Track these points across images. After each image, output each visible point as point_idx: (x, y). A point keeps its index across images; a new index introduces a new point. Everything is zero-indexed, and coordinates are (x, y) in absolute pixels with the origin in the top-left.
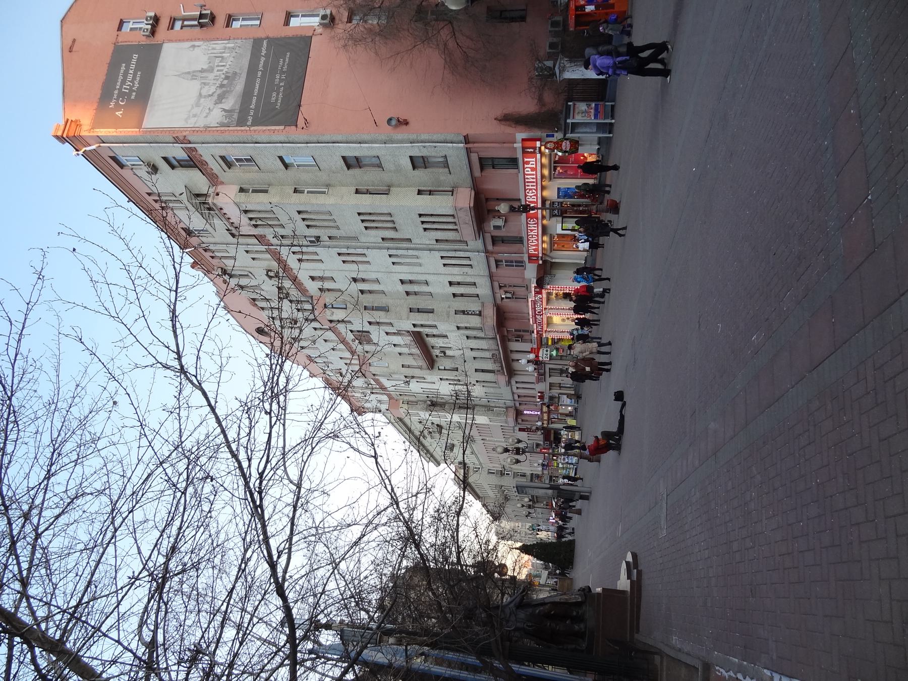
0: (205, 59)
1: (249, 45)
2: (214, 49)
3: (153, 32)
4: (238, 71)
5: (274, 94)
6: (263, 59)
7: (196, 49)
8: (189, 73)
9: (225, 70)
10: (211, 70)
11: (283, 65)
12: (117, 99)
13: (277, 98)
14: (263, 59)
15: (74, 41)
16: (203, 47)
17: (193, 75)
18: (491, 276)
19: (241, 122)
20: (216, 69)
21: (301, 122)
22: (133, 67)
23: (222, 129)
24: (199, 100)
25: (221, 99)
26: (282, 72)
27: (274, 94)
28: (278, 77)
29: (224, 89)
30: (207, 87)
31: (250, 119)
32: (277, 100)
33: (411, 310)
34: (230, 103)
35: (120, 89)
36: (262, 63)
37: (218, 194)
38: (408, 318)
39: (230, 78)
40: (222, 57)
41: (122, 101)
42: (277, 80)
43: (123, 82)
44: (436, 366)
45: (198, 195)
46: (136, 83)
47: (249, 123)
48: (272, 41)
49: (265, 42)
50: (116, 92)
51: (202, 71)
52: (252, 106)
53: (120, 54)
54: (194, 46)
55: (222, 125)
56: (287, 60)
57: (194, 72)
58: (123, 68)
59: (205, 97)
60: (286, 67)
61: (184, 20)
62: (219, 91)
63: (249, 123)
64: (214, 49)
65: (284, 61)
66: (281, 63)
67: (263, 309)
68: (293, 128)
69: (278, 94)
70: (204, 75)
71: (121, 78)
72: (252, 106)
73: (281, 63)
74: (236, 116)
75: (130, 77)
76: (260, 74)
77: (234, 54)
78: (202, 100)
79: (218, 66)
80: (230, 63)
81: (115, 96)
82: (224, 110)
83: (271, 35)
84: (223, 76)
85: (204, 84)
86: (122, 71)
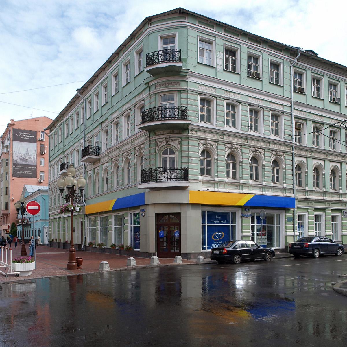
0: (32, 154)
1: (35, 164)
2: (34, 155)
5: (21, 171)
6: (31, 168)
8: (28, 150)
10: (28, 155)
12: (21, 134)
14: (31, 168)
15: (39, 121)
17: (27, 151)
19: (14, 164)
21: (14, 178)
22: (30, 136)
25: (21, 159)
26: (27, 172)
27: (21, 171)
34: (19, 161)
35: (24, 134)
37: (5, 154)
43: (26, 135)
46: (26, 138)
48: (36, 169)
49: (36, 168)
50: (23, 133)
51: (28, 154)
53: (34, 133)
54: (35, 151)
55: (13, 160)
58: (30, 134)
62: (22, 158)
63: (13, 166)
64: (34, 155)
74: (16, 163)
75: (27, 136)
78: (20, 154)
81: (22, 133)
82: (17, 160)
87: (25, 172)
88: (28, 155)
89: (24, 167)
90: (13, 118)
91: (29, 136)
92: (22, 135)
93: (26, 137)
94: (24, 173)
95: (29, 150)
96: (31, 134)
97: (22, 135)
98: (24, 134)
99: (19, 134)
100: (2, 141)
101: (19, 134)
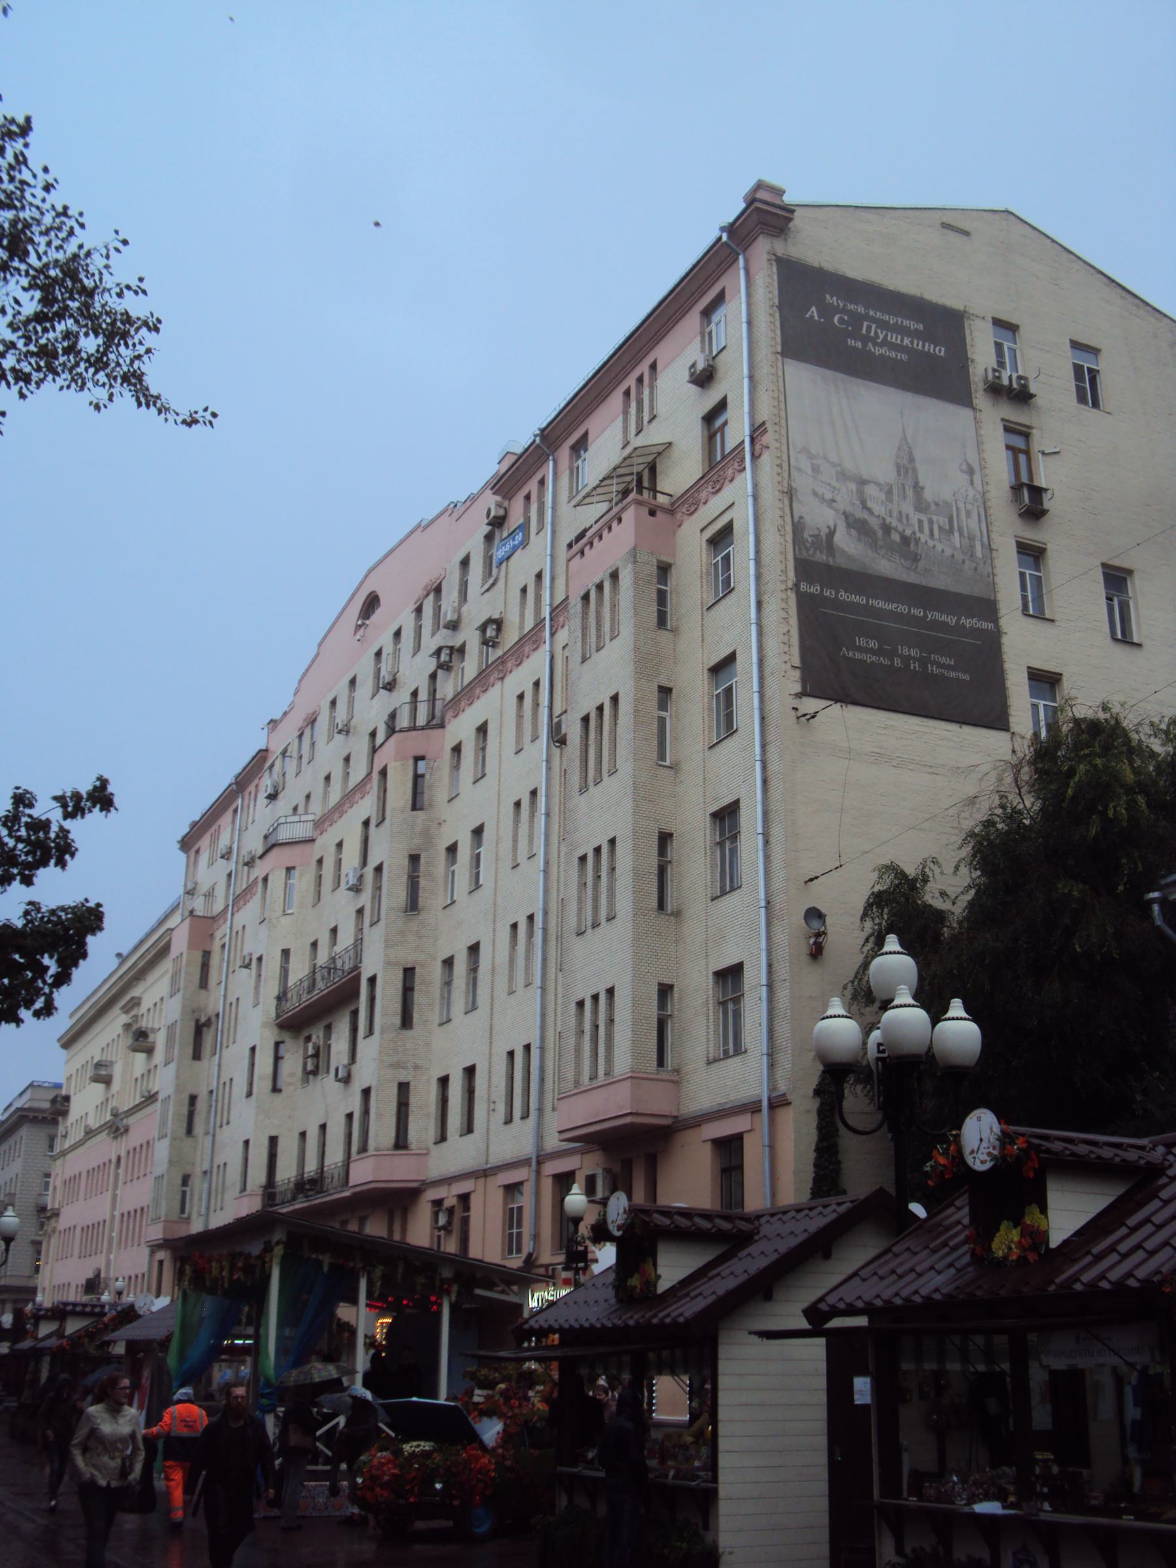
0: (946, 494)
2: (968, 514)
3: (996, 390)
4: (922, 564)
5: (873, 644)
6: (951, 620)
7: (966, 477)
8: (912, 460)
9: (924, 537)
10: (921, 506)
11: (940, 666)
12: (844, 311)
13: (864, 650)
14: (951, 620)
16: (971, 492)
17: (906, 467)
18: (484, 1174)
19: (805, 569)
20: (924, 518)
21: (811, 705)
22: (918, 345)
23: (789, 528)
26: (924, 662)
27: (873, 644)
28: (914, 652)
29: (880, 533)
30: (883, 496)
31: (815, 589)
33: (409, 972)
35: (866, 317)
36: (944, 618)
38: (388, 963)
39: (906, 547)
40: (951, 531)
41: (841, 320)
42: (906, 652)
44: (286, 1037)
45: (653, 468)
46: (883, 351)
47: (803, 586)
50: (861, 309)
51: (918, 489)
52: (843, 595)
53: (946, 324)
54: (971, 472)
56: (953, 674)
57: (915, 470)
60: (936, 671)
61: (1027, 453)
62: (874, 523)
63: (803, 586)
64: (968, 514)
65: (949, 668)
66: (943, 660)
67: (419, 610)
68: (798, 688)
69: (872, 651)
70: (910, 493)
72: (843, 595)
73: (943, 660)
74: (821, 557)
75: (895, 338)
76: (919, 612)
77: (959, 556)
78: (853, 486)
79: (931, 522)
81: (851, 307)
82: (831, 534)
83: (1005, 640)
84: (908, 532)
85: (889, 492)
86: (906, 323)
87: (907, 660)
88: (921, 506)
89: (891, 607)
91: (907, 341)
92: (857, 319)
93: (885, 343)
94: (897, 662)
95: (918, 455)
96: (921, 327)
97: (857, 319)
99: (827, 311)
100: (499, 505)
101: (827, 311)
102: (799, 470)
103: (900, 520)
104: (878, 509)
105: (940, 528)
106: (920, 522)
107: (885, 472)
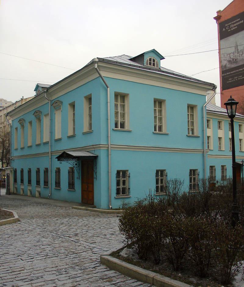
11: (240, 78)
13: (230, 81)
24: (228, 54)
27: (231, 79)
32: (230, 81)
34: (229, 66)
40: (242, 54)
59: (230, 56)
65: (241, 77)
69: (231, 80)
71: (235, 22)
75: (235, 25)
79: (239, 54)
80: (240, 58)
82: (226, 64)
87: (235, 79)
90: (218, 10)
97: (229, 26)
98: (231, 24)
102: (222, 57)
103: (235, 57)
104: (232, 57)
105: (241, 55)
106: (238, 55)
107: (233, 50)
